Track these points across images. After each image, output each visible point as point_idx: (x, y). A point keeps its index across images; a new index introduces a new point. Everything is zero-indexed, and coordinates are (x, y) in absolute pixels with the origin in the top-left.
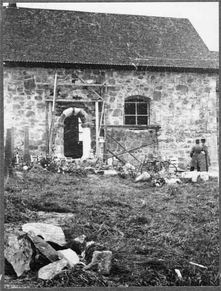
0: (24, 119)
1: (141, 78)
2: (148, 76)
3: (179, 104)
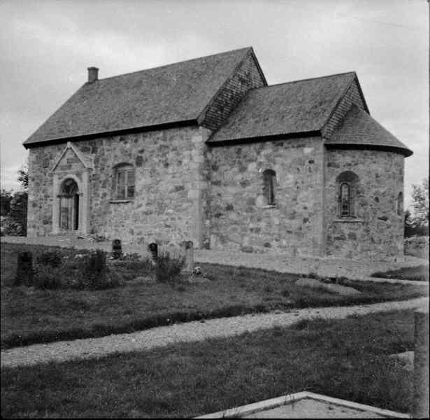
1: (126, 143)
3: (160, 169)
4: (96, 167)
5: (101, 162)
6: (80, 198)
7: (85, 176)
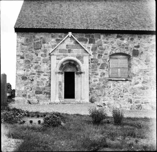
0: (32, 71)
1: (123, 39)
2: (128, 38)
5: (98, 49)
7: (86, 59)
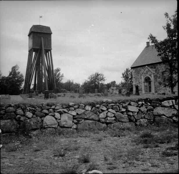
4: (156, 73)
5: (157, 70)
6: (151, 82)
7: (152, 76)
